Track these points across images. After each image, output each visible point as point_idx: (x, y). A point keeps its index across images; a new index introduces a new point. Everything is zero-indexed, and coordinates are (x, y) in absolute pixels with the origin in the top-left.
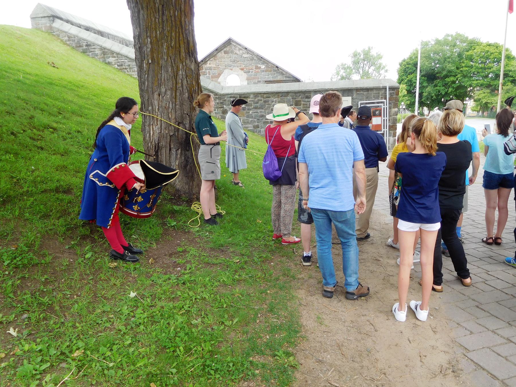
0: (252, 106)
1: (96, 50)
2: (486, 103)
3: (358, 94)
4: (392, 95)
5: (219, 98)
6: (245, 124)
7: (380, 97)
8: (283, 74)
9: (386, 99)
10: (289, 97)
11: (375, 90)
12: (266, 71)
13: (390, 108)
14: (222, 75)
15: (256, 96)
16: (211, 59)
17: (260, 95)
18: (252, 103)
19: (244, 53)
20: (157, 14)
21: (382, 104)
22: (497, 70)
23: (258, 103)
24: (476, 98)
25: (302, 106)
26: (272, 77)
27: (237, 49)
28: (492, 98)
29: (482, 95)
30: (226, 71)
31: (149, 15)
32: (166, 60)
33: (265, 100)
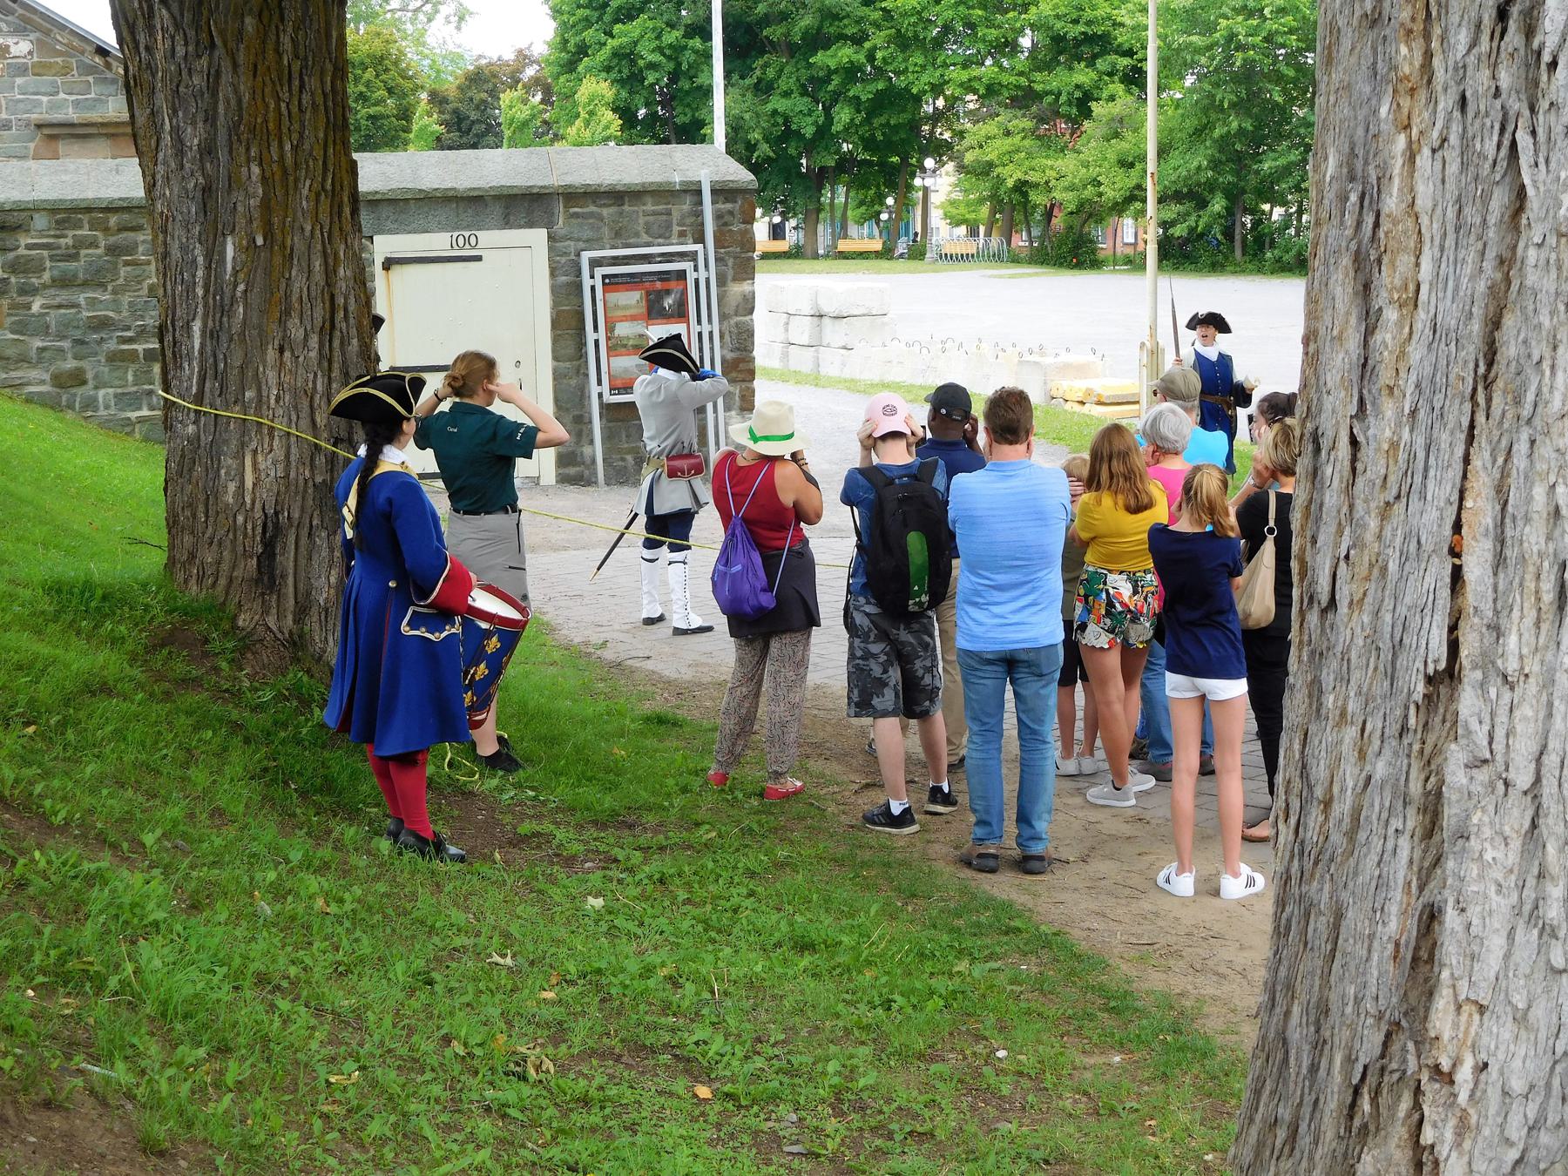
0: (46, 276)
2: (1022, 187)
3: (576, 215)
4: (726, 224)
7: (676, 229)
9: (700, 239)
11: (649, 200)
12: (39, 70)
13: (722, 282)
15: (64, 221)
17: (85, 218)
18: (42, 259)
20: (286, 88)
21: (687, 266)
22: (1058, 17)
23: (74, 257)
24: (969, 157)
26: (76, 104)
28: (1049, 163)
29: (998, 143)
31: (259, 91)
32: (307, 233)
33: (112, 239)
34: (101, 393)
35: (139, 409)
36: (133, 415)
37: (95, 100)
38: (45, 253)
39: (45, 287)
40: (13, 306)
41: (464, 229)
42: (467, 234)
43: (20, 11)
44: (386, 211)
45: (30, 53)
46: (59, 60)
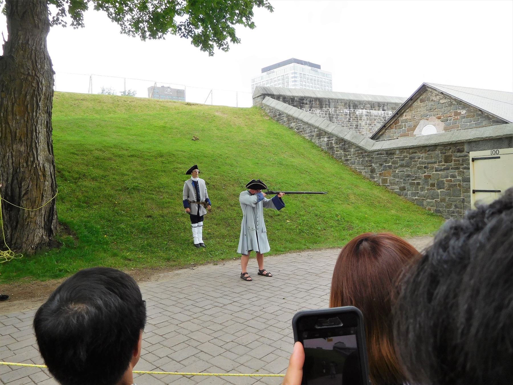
5: (368, 155)
6: (391, 186)
8: (490, 119)
10: (437, 152)
14: (418, 126)
15: (402, 151)
16: (407, 111)
19: (441, 99)
25: (453, 163)
26: (476, 123)
27: (434, 95)
30: (422, 122)
34: (409, 192)
35: (416, 197)
36: (414, 198)
37: (480, 122)
38: (398, 159)
39: (399, 167)
41: (495, 149)
42: (496, 150)
43: (463, 104)
44: (473, 144)
45: (466, 113)
46: (472, 114)
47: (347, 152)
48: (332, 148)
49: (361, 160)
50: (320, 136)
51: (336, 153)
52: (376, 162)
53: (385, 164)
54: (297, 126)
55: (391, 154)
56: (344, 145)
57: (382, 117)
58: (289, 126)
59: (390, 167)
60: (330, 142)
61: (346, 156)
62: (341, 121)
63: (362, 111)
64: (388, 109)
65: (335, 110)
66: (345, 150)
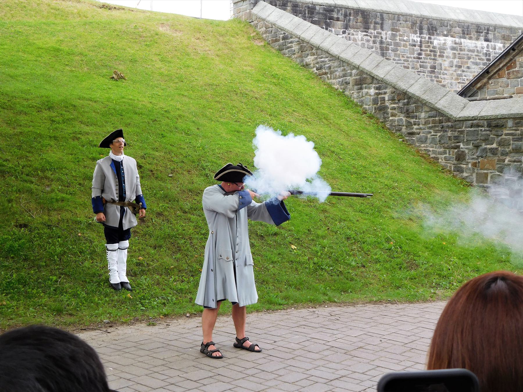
0: (511, 147)
1: (293, 45)
5: (452, 127)
38: (511, 137)
39: (511, 153)
40: (499, 160)
47: (413, 117)
48: (382, 109)
49: (439, 134)
50: (361, 84)
51: (391, 118)
52: (467, 140)
53: (484, 146)
54: (318, 63)
55: (497, 126)
56: (408, 103)
57: (483, 54)
58: (302, 61)
59: (494, 152)
60: (380, 96)
61: (409, 125)
62: (403, 57)
63: (445, 40)
64: (496, 39)
65: (392, 34)
66: (408, 114)
